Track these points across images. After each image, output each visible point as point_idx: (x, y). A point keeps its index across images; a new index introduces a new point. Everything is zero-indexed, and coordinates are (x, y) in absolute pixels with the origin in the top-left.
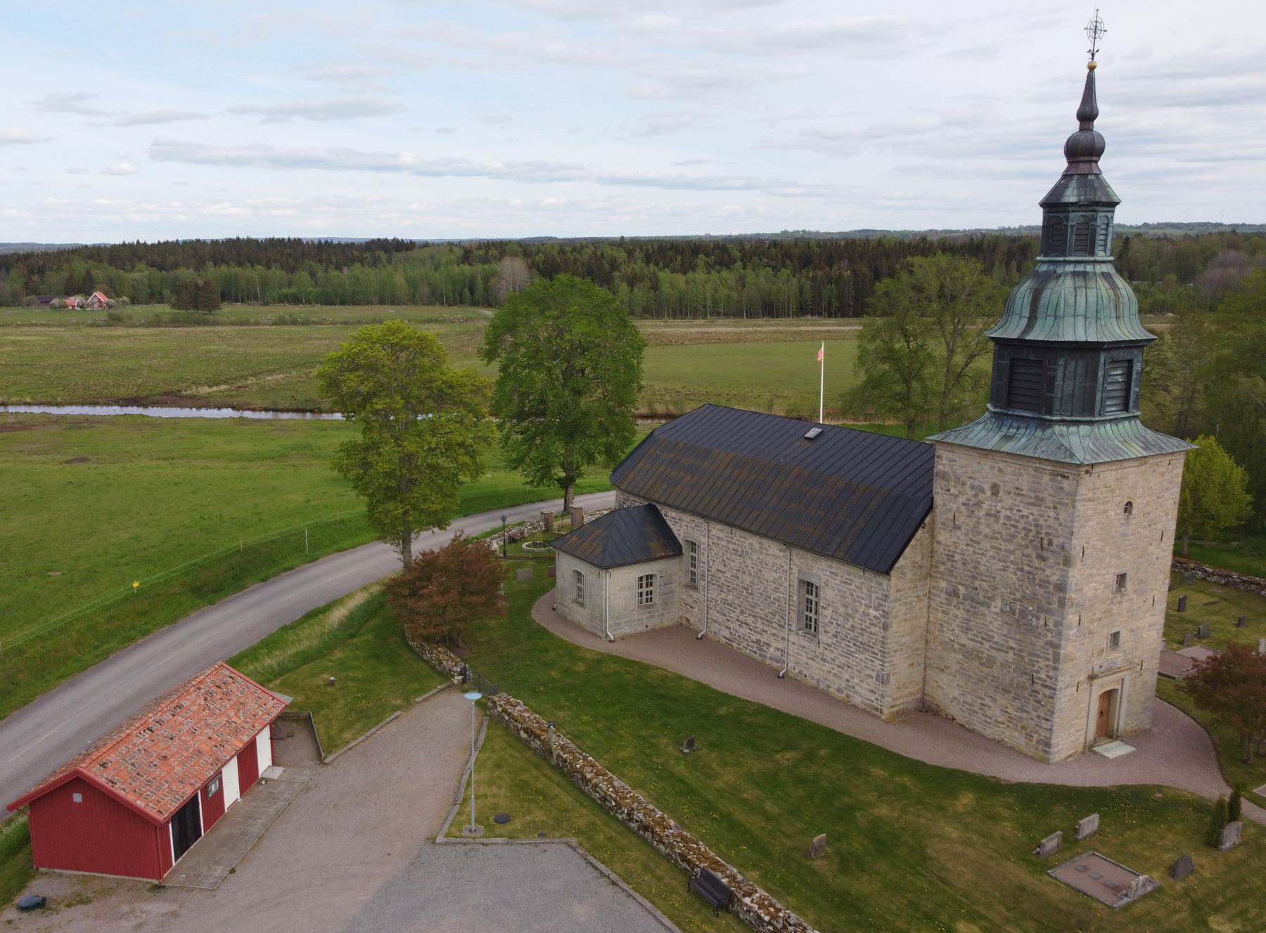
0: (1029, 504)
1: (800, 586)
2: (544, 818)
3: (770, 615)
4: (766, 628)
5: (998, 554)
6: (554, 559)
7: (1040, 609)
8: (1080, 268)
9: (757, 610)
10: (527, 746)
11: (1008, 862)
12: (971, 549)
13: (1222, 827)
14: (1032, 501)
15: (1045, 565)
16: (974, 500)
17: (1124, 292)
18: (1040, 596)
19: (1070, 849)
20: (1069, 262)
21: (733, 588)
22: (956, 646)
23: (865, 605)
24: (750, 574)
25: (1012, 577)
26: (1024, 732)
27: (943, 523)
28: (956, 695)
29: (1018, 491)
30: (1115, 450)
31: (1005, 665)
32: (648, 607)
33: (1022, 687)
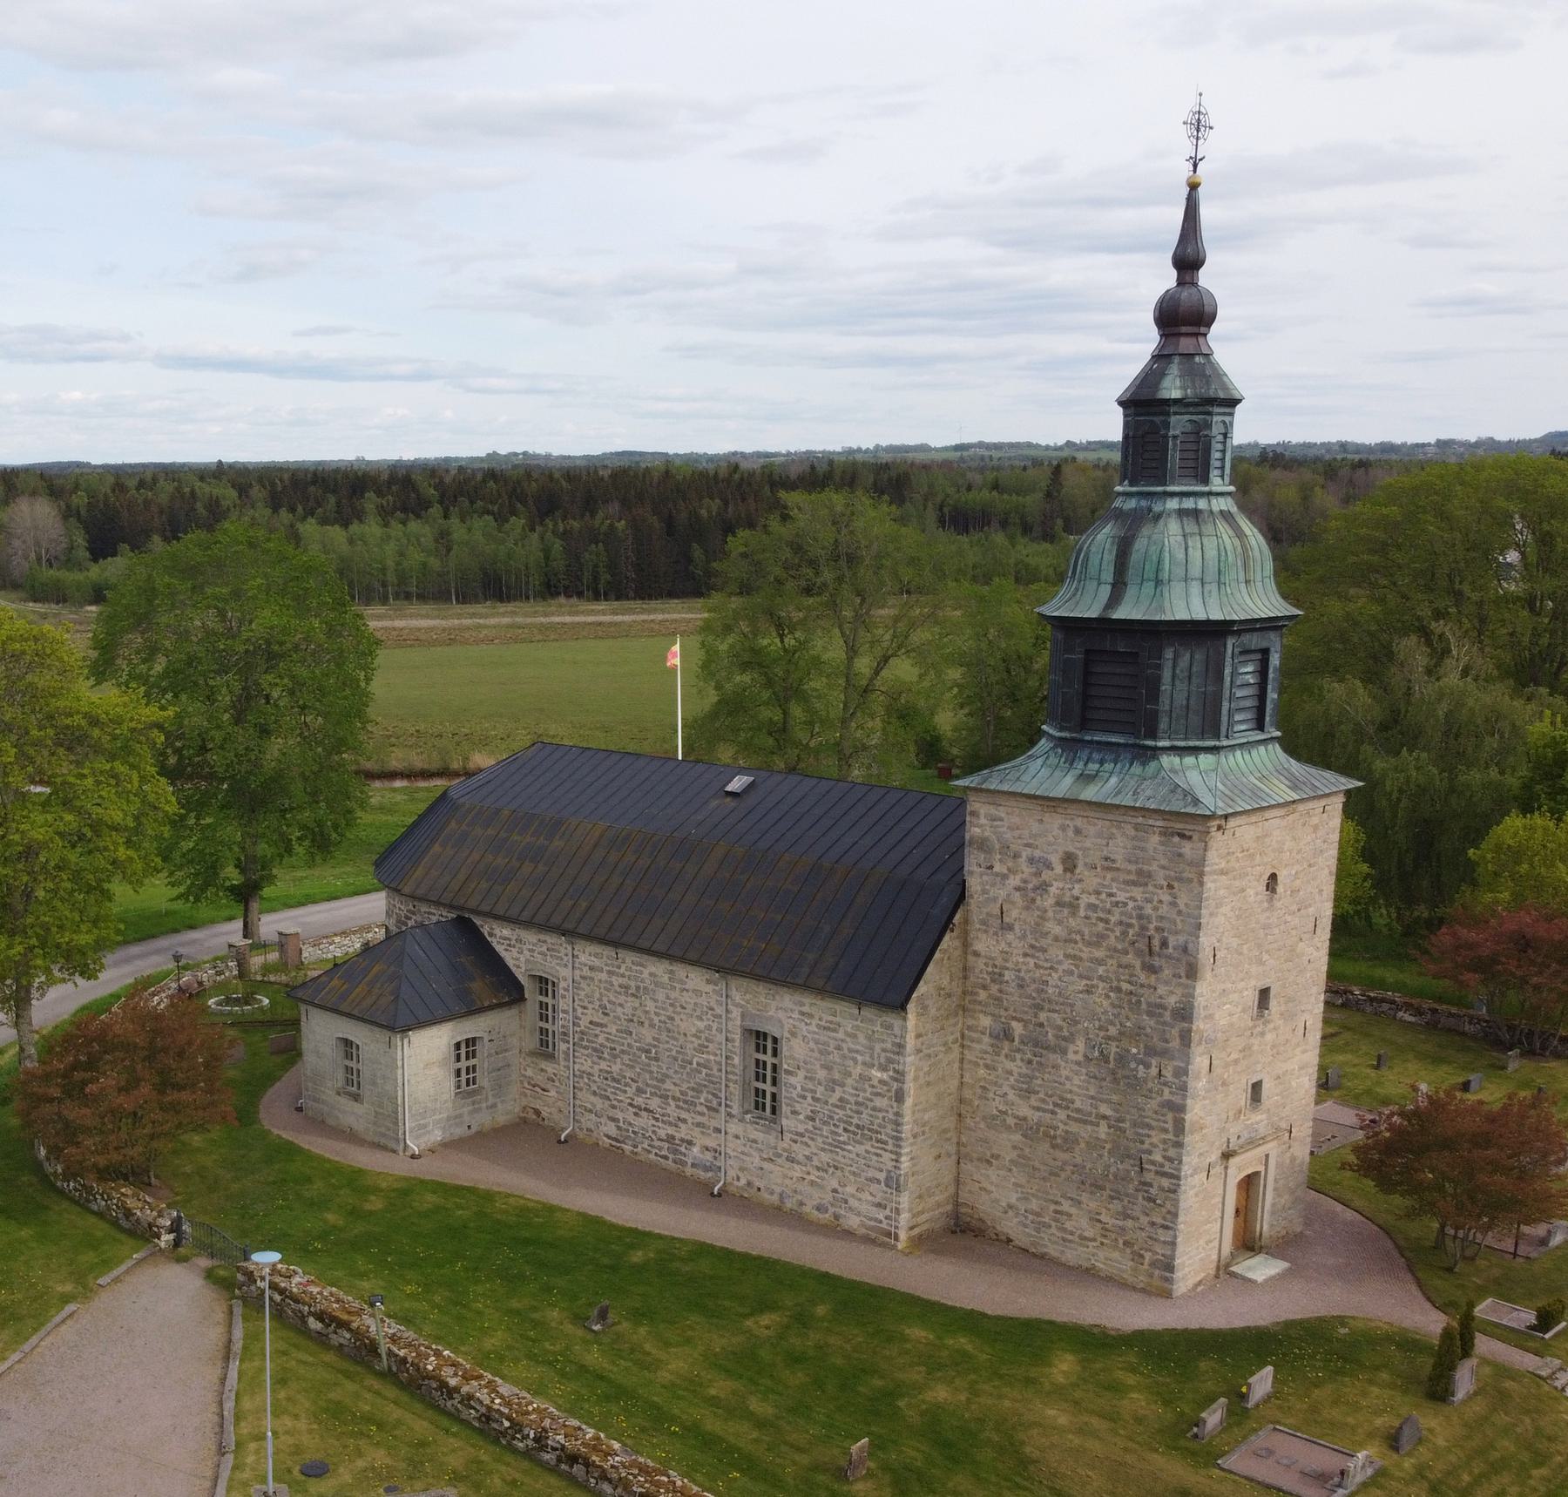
0: (1127, 883)
1: (744, 1041)
2: (388, 1461)
3: (691, 1093)
4: (684, 1115)
5: (1076, 965)
6: (295, 1024)
7: (1151, 1051)
8: (1189, 504)
9: (668, 1085)
10: (324, 1343)
11: (1155, 1456)
12: (1031, 962)
13: (1452, 1368)
14: (1133, 877)
15: (1157, 979)
16: (1035, 882)
17: (1253, 542)
18: (1149, 1030)
19: (1239, 1424)
20: (1172, 495)
21: (623, 1052)
22: (1011, 1121)
23: (864, 1063)
24: (652, 1026)
25: (1101, 1002)
26: (1128, 1251)
27: (984, 922)
28: (1013, 1201)
30: (1255, 793)
31: (1094, 1145)
32: (474, 1092)
33: (1123, 1179)
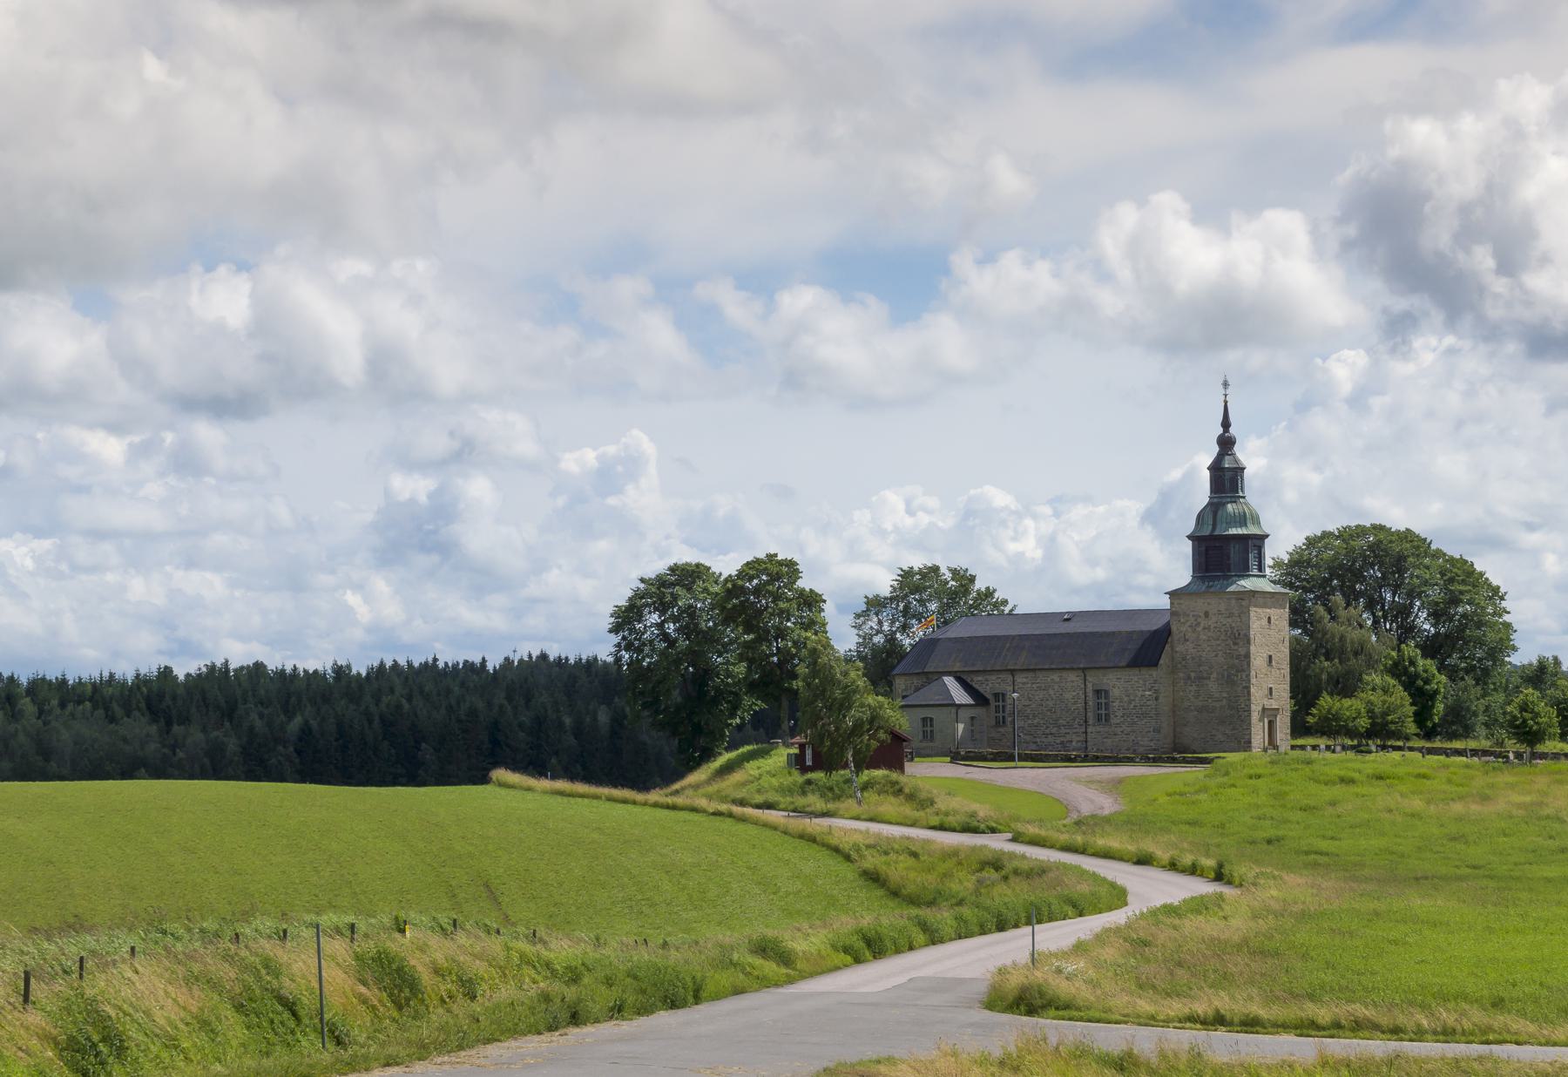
4: (1068, 731)
7: (1238, 671)
16: (1195, 623)
22: (1192, 708)
29: (1219, 612)
